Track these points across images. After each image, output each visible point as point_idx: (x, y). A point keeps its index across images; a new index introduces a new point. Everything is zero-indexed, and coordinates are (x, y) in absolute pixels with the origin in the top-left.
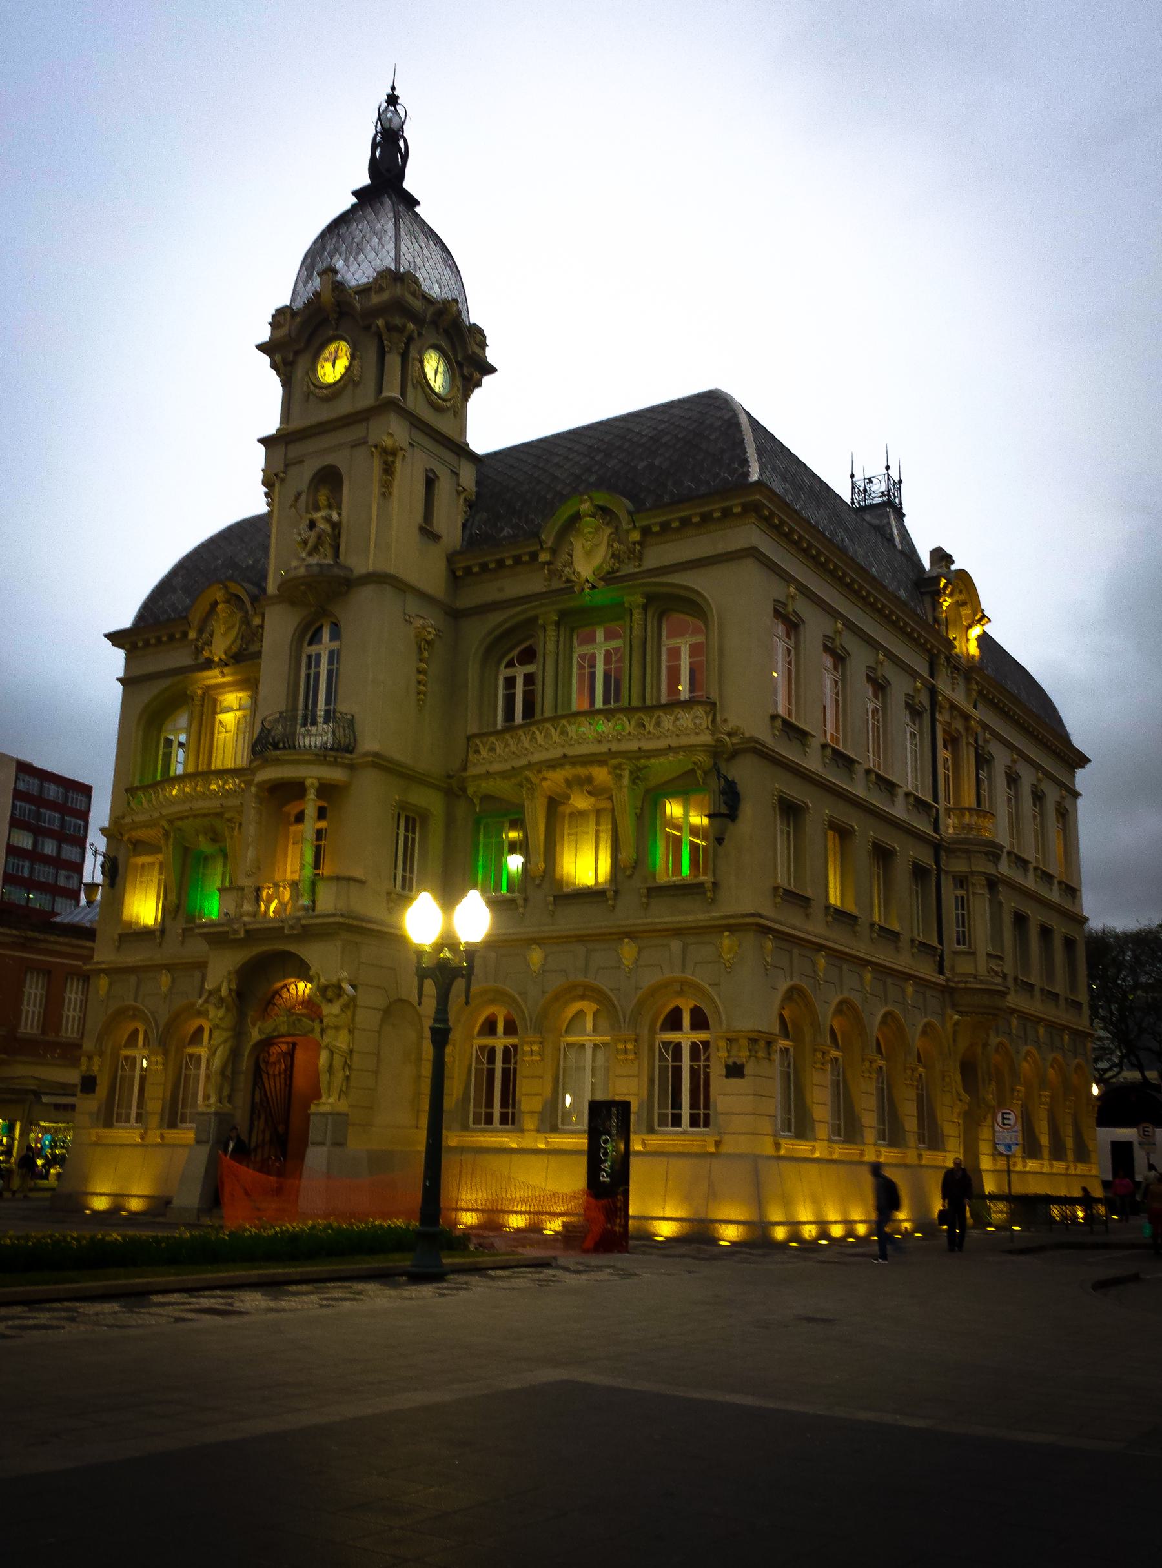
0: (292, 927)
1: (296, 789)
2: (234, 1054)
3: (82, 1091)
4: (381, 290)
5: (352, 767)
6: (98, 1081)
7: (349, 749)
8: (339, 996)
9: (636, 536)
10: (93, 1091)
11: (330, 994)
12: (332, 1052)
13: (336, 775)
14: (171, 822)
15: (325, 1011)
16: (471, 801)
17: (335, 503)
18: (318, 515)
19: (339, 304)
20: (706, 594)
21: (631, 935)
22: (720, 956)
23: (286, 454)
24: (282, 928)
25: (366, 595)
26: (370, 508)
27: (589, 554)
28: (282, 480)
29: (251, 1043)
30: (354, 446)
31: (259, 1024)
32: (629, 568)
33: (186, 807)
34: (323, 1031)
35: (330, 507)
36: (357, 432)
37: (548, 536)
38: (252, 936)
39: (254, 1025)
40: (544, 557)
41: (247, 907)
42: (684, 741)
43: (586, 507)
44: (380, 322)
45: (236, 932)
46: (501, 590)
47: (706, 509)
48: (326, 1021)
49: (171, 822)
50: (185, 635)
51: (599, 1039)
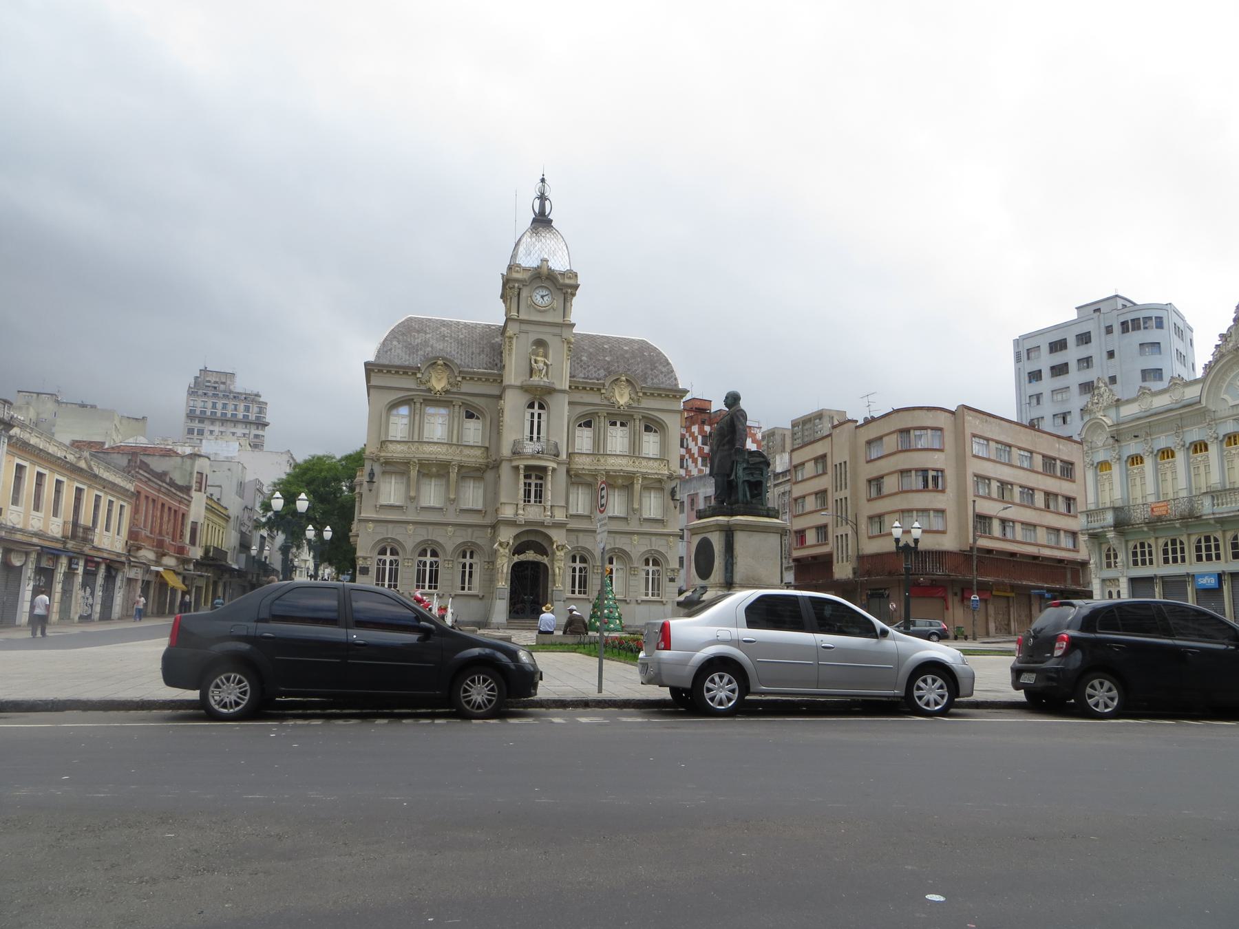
0: (549, 523)
1: (544, 469)
2: (508, 567)
3: (360, 574)
4: (570, 278)
5: (558, 463)
6: (370, 569)
7: (558, 456)
8: (562, 549)
9: (641, 394)
10: (367, 574)
11: (560, 548)
12: (559, 568)
13: (555, 465)
14: (419, 460)
15: (558, 553)
16: (571, 476)
17: (546, 356)
18: (539, 359)
19: (549, 274)
20: (665, 420)
21: (638, 534)
22: (668, 543)
23: (520, 327)
24: (544, 523)
25: (561, 396)
26: (563, 363)
27: (622, 395)
28: (517, 337)
29: (514, 562)
30: (554, 335)
31: (516, 555)
32: (635, 405)
33: (433, 456)
34: (552, 561)
35: (542, 356)
36: (557, 330)
37: (607, 385)
38: (527, 523)
39: (514, 555)
40: (603, 391)
41: (521, 512)
42: (661, 472)
43: (624, 378)
44: (569, 291)
45: (520, 521)
46: (581, 397)
47: (668, 393)
48: (556, 558)
49: (419, 460)
50: (415, 374)
51: (618, 567)
